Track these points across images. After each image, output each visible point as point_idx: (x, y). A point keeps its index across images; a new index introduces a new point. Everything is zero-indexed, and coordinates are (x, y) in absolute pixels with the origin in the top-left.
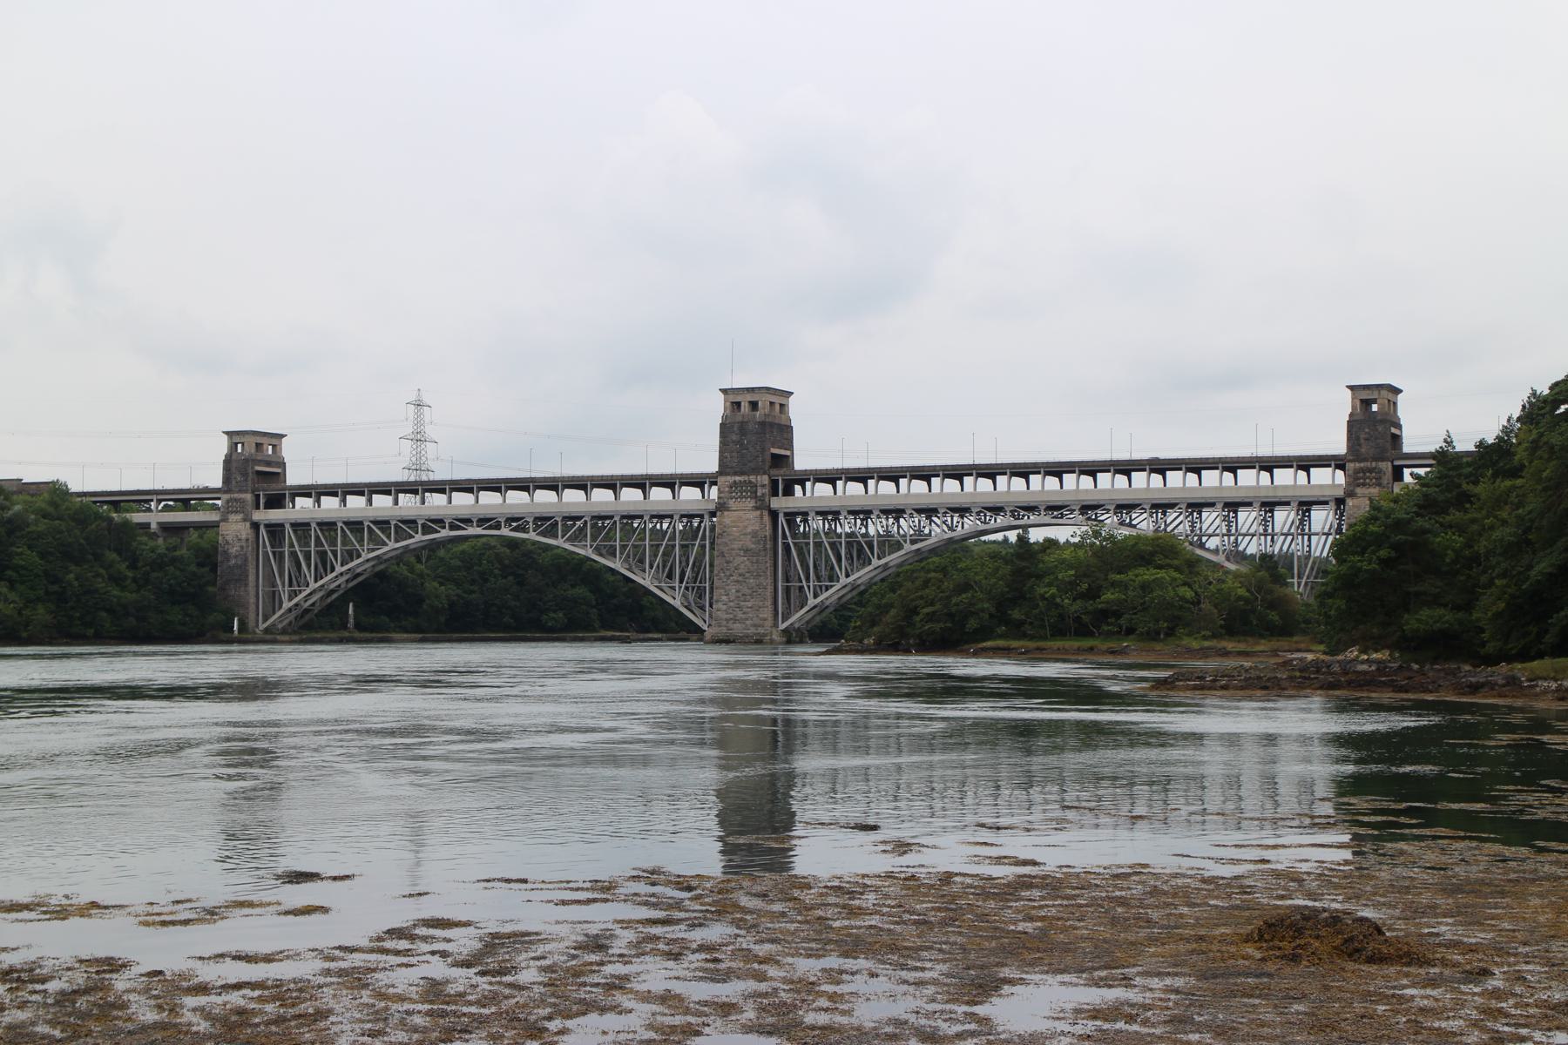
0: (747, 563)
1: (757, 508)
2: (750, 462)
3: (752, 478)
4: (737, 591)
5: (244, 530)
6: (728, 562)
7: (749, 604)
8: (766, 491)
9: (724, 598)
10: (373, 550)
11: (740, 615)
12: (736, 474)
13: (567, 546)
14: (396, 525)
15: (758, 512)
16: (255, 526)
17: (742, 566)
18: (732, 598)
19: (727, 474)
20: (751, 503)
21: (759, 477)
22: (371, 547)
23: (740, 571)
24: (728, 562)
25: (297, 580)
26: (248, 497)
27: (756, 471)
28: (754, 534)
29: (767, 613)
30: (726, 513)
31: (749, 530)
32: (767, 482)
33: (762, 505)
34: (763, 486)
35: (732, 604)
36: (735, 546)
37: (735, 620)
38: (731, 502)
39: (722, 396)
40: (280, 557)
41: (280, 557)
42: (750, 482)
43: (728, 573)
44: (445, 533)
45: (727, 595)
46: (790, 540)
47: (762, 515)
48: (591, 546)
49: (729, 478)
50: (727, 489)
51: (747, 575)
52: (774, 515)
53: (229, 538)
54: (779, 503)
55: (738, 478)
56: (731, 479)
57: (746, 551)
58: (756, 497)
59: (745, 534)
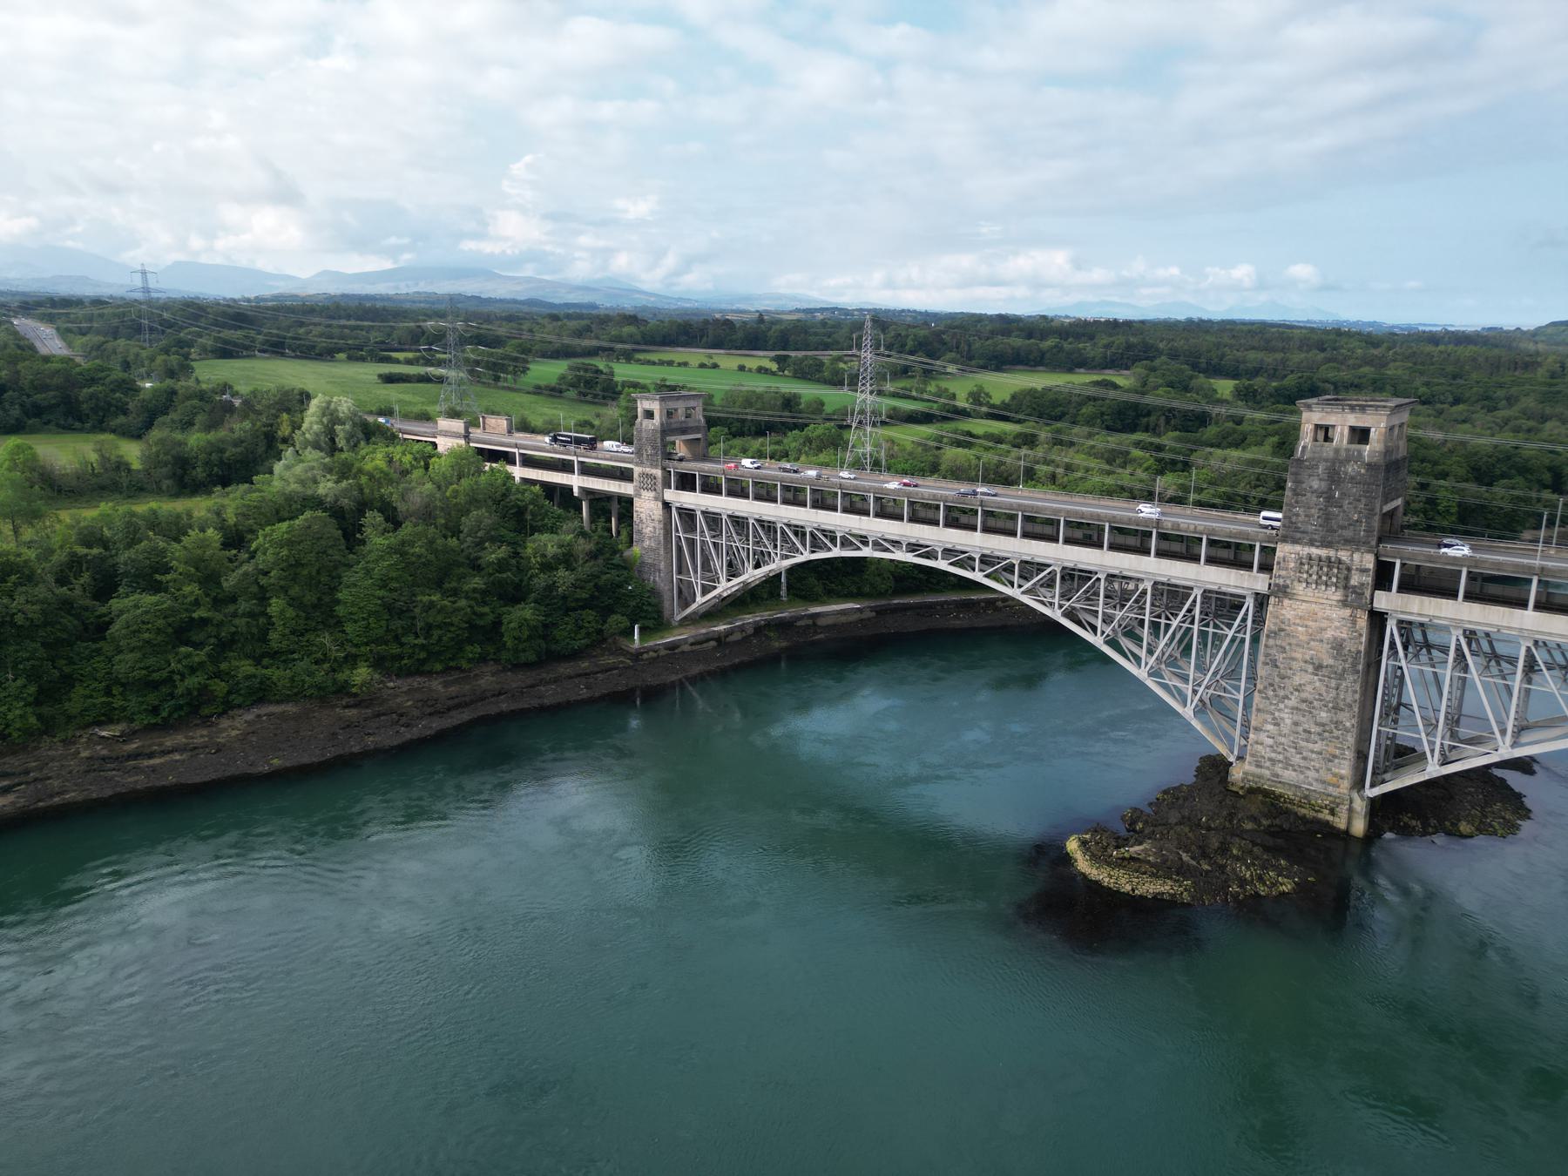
0: (1318, 684)
1: (1344, 603)
2: (1343, 528)
3: (1344, 555)
4: (1296, 724)
5: (657, 510)
6: (1283, 677)
7: (1317, 747)
8: (1368, 579)
9: (1270, 727)
10: (787, 557)
11: (1297, 759)
12: (1311, 543)
14: (811, 533)
15: (1348, 612)
16: (667, 506)
17: (1309, 688)
18: (1286, 731)
19: (1295, 541)
21: (1356, 556)
22: (784, 553)
23: (1304, 695)
24: (1283, 677)
27: (1354, 543)
28: (1338, 646)
29: (1345, 768)
30: (1286, 602)
31: (1329, 634)
32: (1371, 566)
34: (1364, 571)
35: (1283, 740)
36: (1299, 656)
37: (1287, 764)
38: (1300, 588)
42: (1340, 562)
43: (1282, 693)
44: (867, 552)
48: (1061, 606)
49: (1298, 548)
51: (1316, 703)
52: (1378, 620)
53: (643, 516)
55: (1315, 551)
57: (1318, 667)
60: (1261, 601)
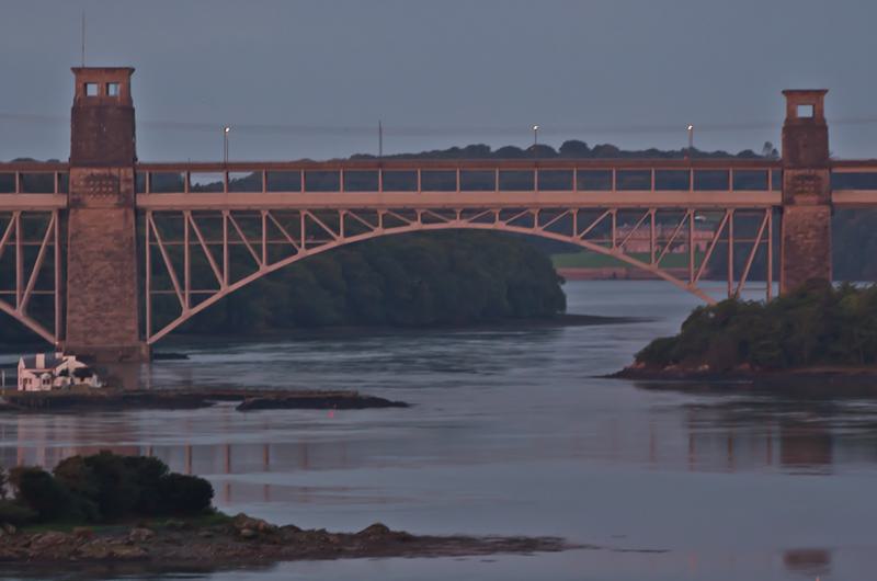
0: (110, 268)
1: (119, 206)
3: (114, 171)
4: (98, 300)
15: (122, 211)
20: (113, 200)
28: (117, 235)
30: (81, 211)
33: (127, 202)
34: (127, 181)
38: (89, 200)
39: (73, 76)
45: (85, 304)
46: (160, 243)
47: (126, 215)
49: (84, 170)
50: (82, 183)
51: (110, 282)
52: (139, 213)
54: (144, 200)
55: (96, 171)
56: (87, 172)
58: (119, 193)
59: (106, 235)
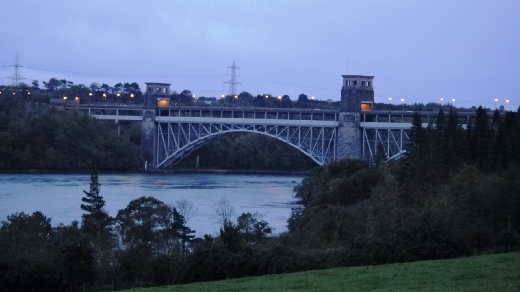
5: (152, 125)
13: (280, 138)
20: (352, 124)
25: (173, 148)
26: (154, 111)
28: (353, 137)
38: (345, 124)
40: (166, 137)
41: (166, 137)
52: (361, 129)
60: (337, 128)
